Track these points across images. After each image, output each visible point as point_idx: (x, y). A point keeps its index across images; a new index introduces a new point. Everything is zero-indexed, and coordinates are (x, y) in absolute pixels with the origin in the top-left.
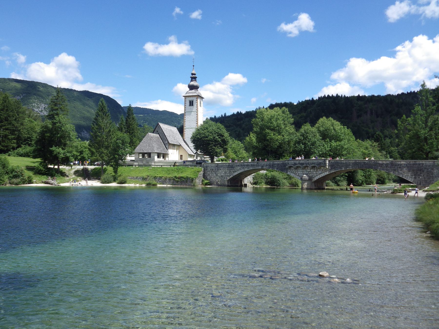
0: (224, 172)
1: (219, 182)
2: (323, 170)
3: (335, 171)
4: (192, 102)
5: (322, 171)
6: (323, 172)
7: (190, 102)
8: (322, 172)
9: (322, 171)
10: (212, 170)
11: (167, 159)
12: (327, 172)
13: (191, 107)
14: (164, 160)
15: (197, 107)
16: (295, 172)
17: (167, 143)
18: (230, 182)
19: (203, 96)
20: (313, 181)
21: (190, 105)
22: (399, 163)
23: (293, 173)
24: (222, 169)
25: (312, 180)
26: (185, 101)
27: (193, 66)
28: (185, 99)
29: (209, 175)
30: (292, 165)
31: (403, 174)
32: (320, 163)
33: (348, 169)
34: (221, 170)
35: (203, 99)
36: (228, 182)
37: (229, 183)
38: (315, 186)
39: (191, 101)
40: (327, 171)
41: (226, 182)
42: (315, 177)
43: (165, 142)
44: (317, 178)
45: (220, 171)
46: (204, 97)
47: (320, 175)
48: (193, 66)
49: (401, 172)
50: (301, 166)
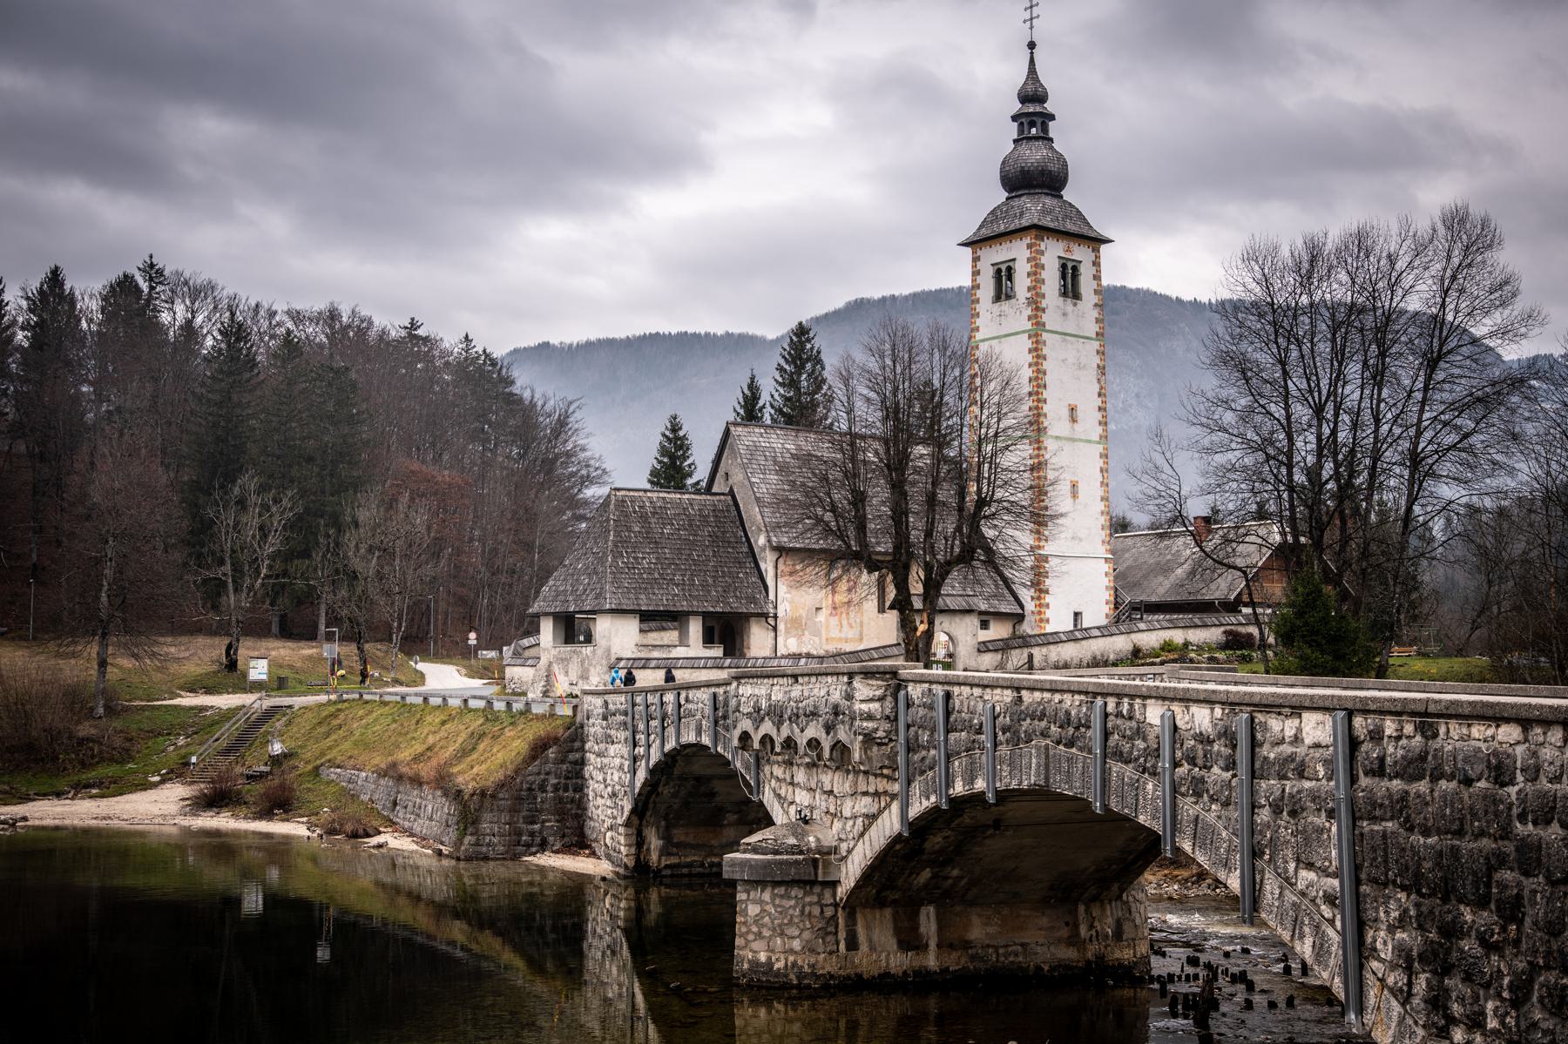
0: (617, 761)
1: (609, 834)
2: (882, 785)
3: (926, 804)
4: (1009, 269)
5: (877, 794)
6: (881, 812)
7: (999, 271)
8: (877, 806)
9: (877, 794)
10: (597, 743)
11: (759, 642)
12: (895, 806)
13: (1005, 306)
14: (717, 652)
15: (1036, 304)
16: (783, 792)
17: (763, 549)
18: (666, 837)
19: (1101, 227)
20: (841, 891)
21: (998, 298)
22: (1290, 727)
23: (778, 796)
24: (613, 732)
25: (834, 884)
26: (976, 273)
27: (1032, 45)
28: (976, 259)
29: (592, 779)
30: (746, 725)
31: (1327, 911)
32: (836, 711)
33: (980, 785)
34: (613, 743)
35: (1103, 248)
36: (639, 842)
37: (654, 842)
38: (909, 940)
39: (1004, 267)
40: (893, 797)
41: (622, 842)
42: (849, 851)
43: (756, 541)
44: (858, 873)
45: (612, 749)
46: (1106, 234)
47: (866, 837)
48: (1032, 45)
49: (1306, 876)
50: (774, 734)
